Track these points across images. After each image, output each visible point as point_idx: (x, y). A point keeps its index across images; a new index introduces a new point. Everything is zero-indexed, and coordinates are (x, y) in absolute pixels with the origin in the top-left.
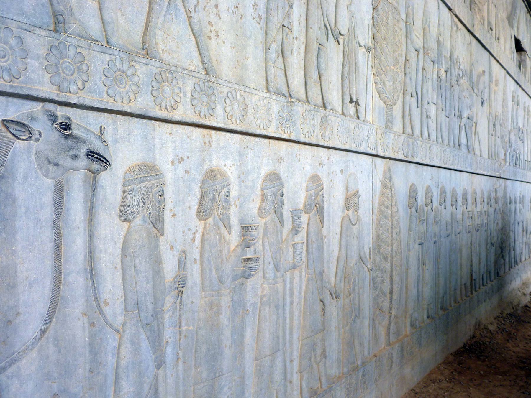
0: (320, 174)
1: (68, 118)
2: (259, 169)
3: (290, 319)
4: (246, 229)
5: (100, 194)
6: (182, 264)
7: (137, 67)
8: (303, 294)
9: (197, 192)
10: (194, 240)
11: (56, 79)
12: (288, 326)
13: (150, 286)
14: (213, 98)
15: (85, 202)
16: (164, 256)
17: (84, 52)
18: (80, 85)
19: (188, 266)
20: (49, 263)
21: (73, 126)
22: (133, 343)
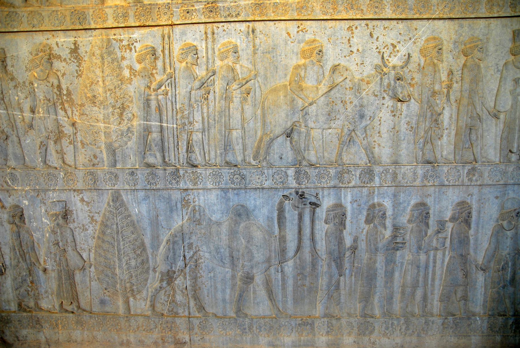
0: (469, 201)
1: (303, 192)
2: (409, 201)
3: (432, 274)
4: (396, 228)
5: (316, 215)
6: (355, 240)
7: (331, 171)
8: (446, 263)
9: (365, 213)
10: (362, 232)
11: (298, 181)
12: (430, 277)
13: (337, 247)
14: (373, 175)
15: (310, 218)
16: (345, 237)
17: (307, 171)
18: (306, 181)
19: (359, 243)
20: (296, 236)
21: (305, 194)
22: (328, 265)
